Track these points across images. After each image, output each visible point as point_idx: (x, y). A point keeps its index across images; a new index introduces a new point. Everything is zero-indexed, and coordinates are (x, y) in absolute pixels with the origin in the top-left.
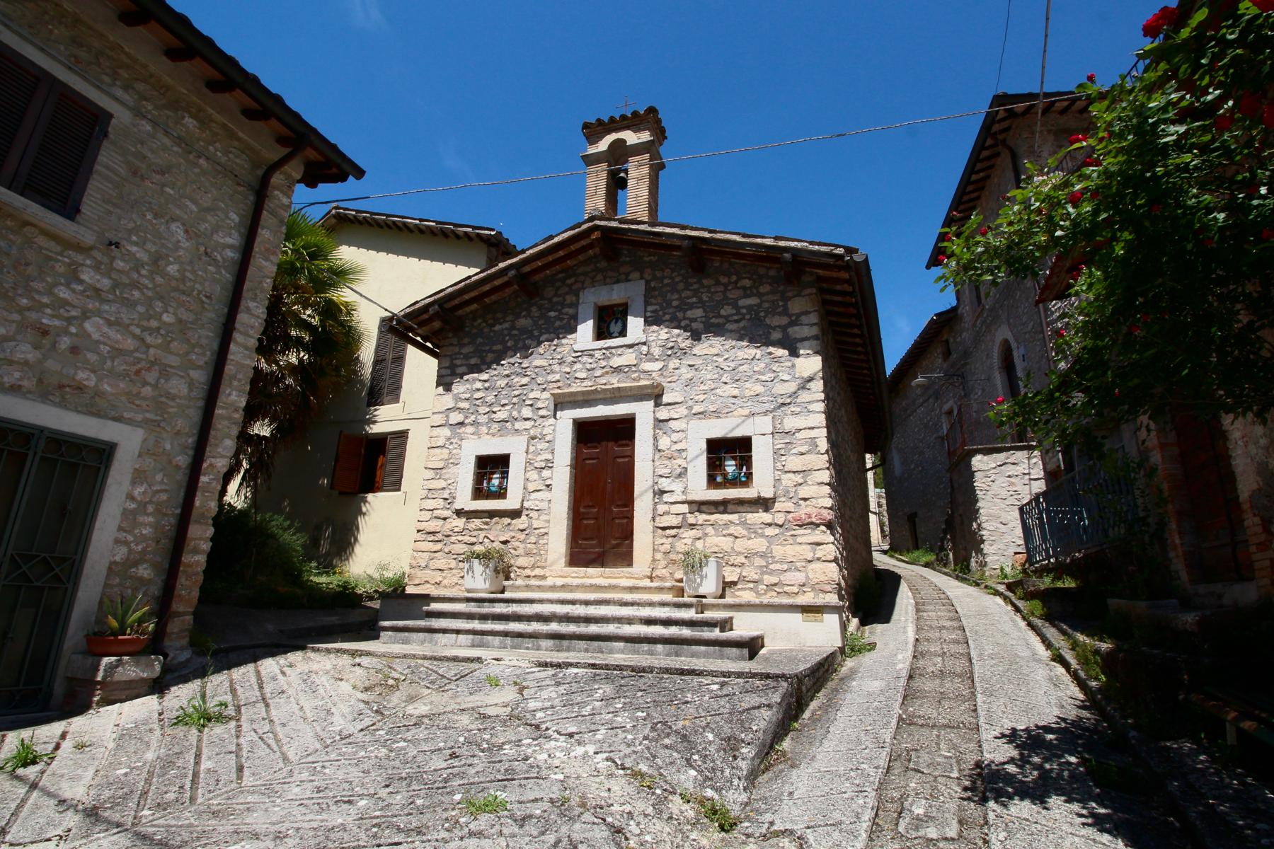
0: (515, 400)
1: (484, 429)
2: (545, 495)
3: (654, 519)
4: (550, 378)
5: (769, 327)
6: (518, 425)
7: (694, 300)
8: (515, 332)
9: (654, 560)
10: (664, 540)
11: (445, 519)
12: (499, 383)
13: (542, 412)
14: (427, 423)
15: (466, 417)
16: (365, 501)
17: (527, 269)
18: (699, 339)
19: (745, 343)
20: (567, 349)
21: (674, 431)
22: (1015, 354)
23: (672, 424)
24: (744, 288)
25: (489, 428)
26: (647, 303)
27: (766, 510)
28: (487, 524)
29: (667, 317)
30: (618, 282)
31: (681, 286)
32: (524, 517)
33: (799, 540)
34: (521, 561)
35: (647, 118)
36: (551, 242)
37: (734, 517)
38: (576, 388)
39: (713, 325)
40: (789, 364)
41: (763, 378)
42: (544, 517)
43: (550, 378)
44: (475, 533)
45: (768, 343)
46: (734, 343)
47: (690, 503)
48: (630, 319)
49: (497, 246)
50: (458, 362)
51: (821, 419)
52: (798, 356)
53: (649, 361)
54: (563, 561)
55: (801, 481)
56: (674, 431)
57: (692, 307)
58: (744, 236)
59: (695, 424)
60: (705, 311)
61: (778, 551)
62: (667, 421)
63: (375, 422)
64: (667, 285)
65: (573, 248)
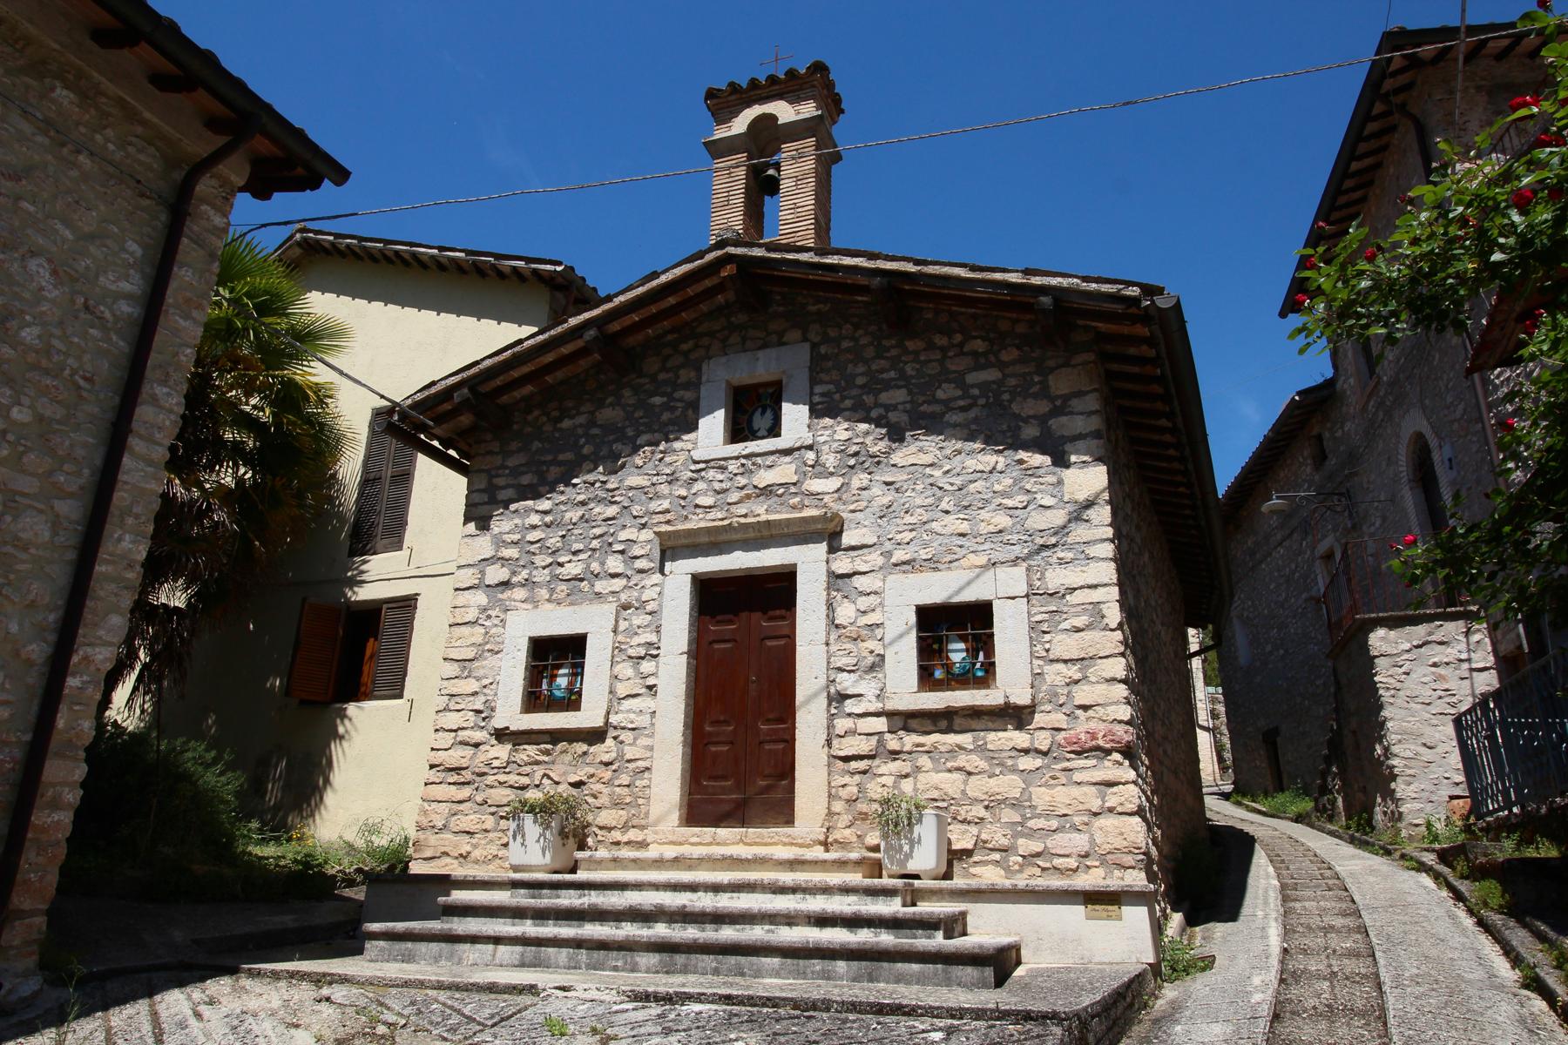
0: (595, 544)
2: (645, 703)
3: (829, 743)
4: (654, 506)
5: (1017, 417)
6: (600, 586)
7: (892, 374)
8: (595, 431)
9: (830, 814)
10: (847, 779)
11: (477, 745)
12: (568, 515)
13: (640, 564)
15: (514, 573)
16: (343, 715)
17: (615, 327)
18: (901, 440)
19: (978, 445)
20: (682, 457)
21: (862, 594)
22: (1436, 456)
23: (858, 582)
24: (975, 354)
25: (552, 591)
26: (813, 382)
27: (1020, 726)
28: (547, 753)
29: (848, 403)
30: (765, 346)
31: (870, 352)
32: (609, 742)
33: (1077, 777)
34: (605, 817)
35: (809, 80)
37: (965, 739)
38: (696, 522)
39: (924, 416)
40: (1051, 479)
41: (1010, 503)
42: (643, 741)
43: (654, 506)
44: (528, 769)
45: (1015, 446)
46: (959, 445)
47: (890, 715)
48: (786, 407)
49: (566, 290)
50: (500, 481)
51: (1108, 572)
52: (1067, 465)
53: (818, 476)
54: (675, 817)
55: (1078, 676)
56: (862, 594)
57: (888, 386)
58: (973, 268)
59: (896, 580)
60: (910, 393)
61: (1041, 796)
62: (849, 576)
64: (848, 350)
65: (690, 292)
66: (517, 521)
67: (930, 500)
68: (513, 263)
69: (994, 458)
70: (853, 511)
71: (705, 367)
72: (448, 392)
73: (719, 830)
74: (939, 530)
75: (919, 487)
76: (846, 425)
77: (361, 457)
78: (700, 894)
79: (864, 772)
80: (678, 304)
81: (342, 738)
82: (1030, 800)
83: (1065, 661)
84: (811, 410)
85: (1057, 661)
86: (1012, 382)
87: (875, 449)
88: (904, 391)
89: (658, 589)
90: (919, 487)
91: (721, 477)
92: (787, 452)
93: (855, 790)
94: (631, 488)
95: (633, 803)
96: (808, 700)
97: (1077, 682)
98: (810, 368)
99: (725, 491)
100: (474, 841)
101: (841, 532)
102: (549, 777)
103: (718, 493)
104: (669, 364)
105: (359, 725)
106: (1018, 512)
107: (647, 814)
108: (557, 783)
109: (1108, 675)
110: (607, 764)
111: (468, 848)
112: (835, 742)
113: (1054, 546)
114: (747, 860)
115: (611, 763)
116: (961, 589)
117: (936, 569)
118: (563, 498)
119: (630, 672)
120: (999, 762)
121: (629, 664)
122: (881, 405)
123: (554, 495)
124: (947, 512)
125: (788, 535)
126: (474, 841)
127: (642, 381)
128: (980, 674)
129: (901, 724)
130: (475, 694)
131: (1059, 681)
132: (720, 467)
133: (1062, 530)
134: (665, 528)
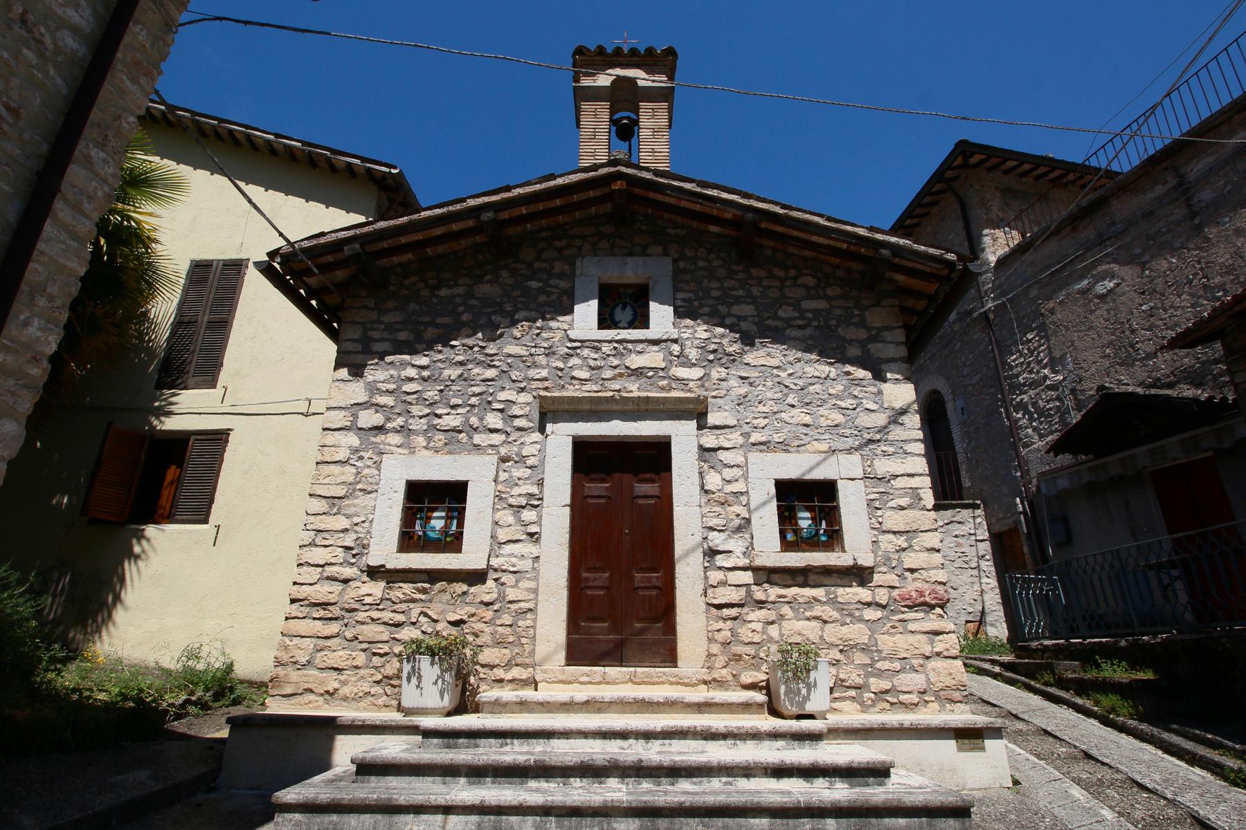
0: (474, 400)
1: (421, 441)
2: (529, 549)
4: (532, 373)
5: (843, 339)
6: (478, 439)
7: (741, 292)
9: (710, 655)
10: (720, 625)
11: (346, 581)
12: (446, 373)
14: (316, 423)
15: (388, 419)
16: (141, 536)
17: (505, 215)
18: (752, 345)
19: (814, 357)
20: (559, 335)
21: (726, 466)
22: (949, 406)
23: (722, 455)
24: (806, 286)
25: (429, 439)
26: (676, 289)
28: (424, 591)
29: (706, 310)
30: (631, 254)
31: (721, 273)
32: (490, 583)
33: (911, 627)
34: (486, 656)
36: (552, 183)
37: (819, 592)
38: (571, 392)
39: (769, 328)
40: (874, 390)
41: (843, 404)
43: (532, 373)
44: (404, 606)
45: (844, 360)
46: (799, 354)
47: (756, 570)
48: (654, 306)
49: (390, 193)
51: (921, 465)
52: (885, 380)
53: (683, 365)
54: (562, 655)
55: (905, 545)
56: (726, 466)
57: (738, 301)
58: (829, 219)
59: (755, 457)
60: (757, 309)
61: (886, 642)
62: (714, 450)
63: (171, 413)
64: (702, 268)
65: (575, 198)
66: (392, 372)
67: (779, 395)
68: (349, 159)
69: (827, 368)
70: (715, 397)
72: (338, 245)
73: (608, 669)
74: (788, 420)
75: (769, 384)
76: (705, 327)
77: (176, 301)
78: (631, 741)
79: (735, 619)
80: (562, 207)
81: (137, 557)
82: (876, 644)
83: (895, 533)
84: (675, 312)
85: (889, 532)
86: (838, 312)
87: (731, 349)
88: (752, 307)
89: (538, 447)
90: (769, 384)
91: (596, 356)
92: (656, 342)
93: (729, 634)
94: (510, 356)
95: (519, 642)
96: (687, 554)
97: (904, 550)
100: (342, 678)
101: (706, 413)
102: (426, 615)
103: (592, 368)
104: (544, 256)
105: (156, 546)
106: (849, 412)
108: (436, 621)
109: (929, 545)
110: (487, 604)
111: (336, 685)
112: (710, 591)
113: (879, 441)
114: (658, 703)
115: (492, 604)
116: (812, 469)
117: (787, 451)
118: (441, 357)
119: (511, 519)
120: (848, 613)
121: (509, 511)
122: (733, 316)
123: (431, 353)
124: (793, 406)
125: (662, 411)
127: (519, 266)
128: (823, 538)
129: (765, 578)
131: (891, 548)
132: (593, 348)
133: (883, 429)
134: (543, 393)
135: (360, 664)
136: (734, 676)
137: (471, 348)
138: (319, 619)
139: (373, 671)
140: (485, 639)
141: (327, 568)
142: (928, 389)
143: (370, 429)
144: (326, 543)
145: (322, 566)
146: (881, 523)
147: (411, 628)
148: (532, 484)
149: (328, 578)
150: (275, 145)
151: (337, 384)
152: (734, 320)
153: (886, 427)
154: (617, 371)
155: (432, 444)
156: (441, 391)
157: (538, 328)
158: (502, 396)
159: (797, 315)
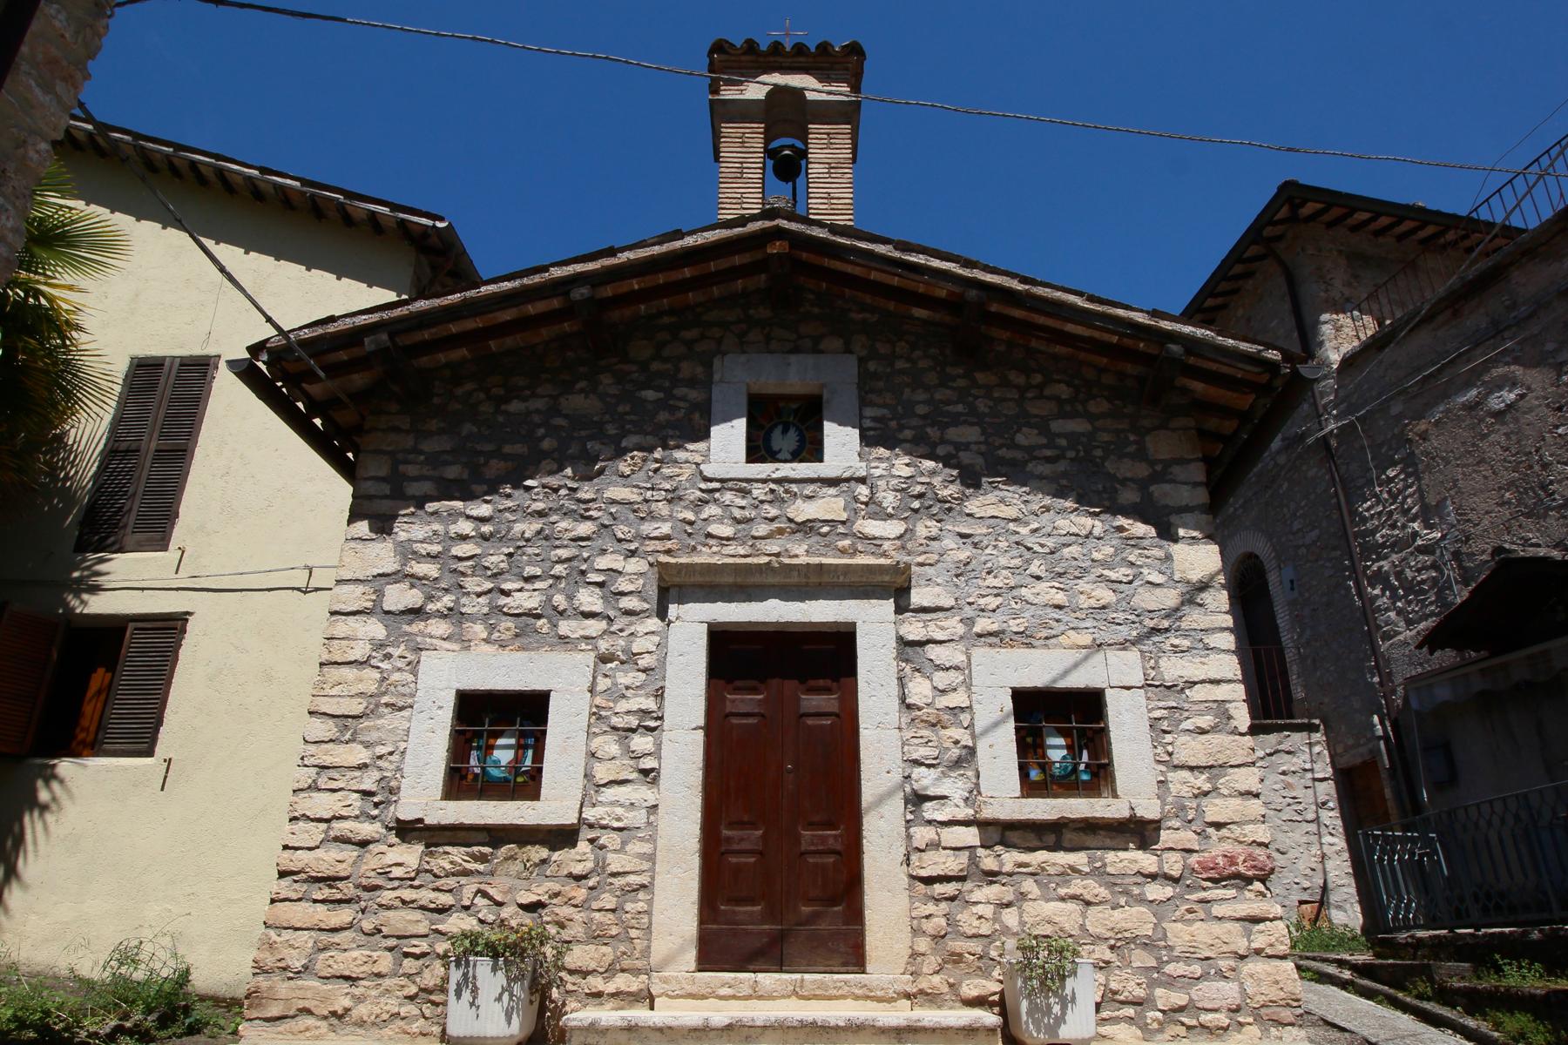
0: (559, 569)
1: (479, 630)
2: (641, 793)
3: (908, 862)
4: (647, 528)
5: (1112, 477)
6: (565, 627)
7: (960, 408)
8: (560, 421)
9: (914, 955)
10: (931, 908)
11: (363, 844)
12: (518, 527)
13: (625, 603)
14: (319, 604)
16: (50, 776)
17: (608, 291)
19: (1069, 504)
20: (687, 471)
21: (939, 668)
22: (1272, 578)
23: (933, 652)
24: (1057, 399)
25: (492, 628)
26: (863, 402)
27: (1144, 845)
28: (483, 858)
29: (908, 434)
30: (796, 350)
31: (932, 378)
32: (583, 846)
33: (1217, 910)
34: (578, 956)
35: (840, 61)
36: (678, 244)
37: (1079, 859)
38: (704, 557)
39: (1002, 461)
40: (1159, 553)
41: (1113, 575)
42: (637, 847)
43: (647, 528)
44: (451, 882)
45: (1114, 509)
46: (1048, 501)
47: (983, 825)
48: (830, 428)
49: (433, 257)
50: (412, 470)
51: (1230, 666)
52: (1175, 539)
53: (873, 516)
54: (691, 955)
55: (1207, 787)
56: (939, 668)
57: (956, 420)
58: (1091, 299)
59: (982, 655)
61: (1179, 934)
63: (95, 589)
64: (902, 372)
65: (712, 266)
66: (436, 526)
67: (1017, 562)
68: (372, 207)
69: (1089, 521)
70: (921, 565)
71: (717, 363)
73: (760, 976)
75: (1003, 545)
76: (907, 460)
77: (108, 418)
79: (952, 899)
80: (693, 279)
81: (44, 808)
82: (1165, 937)
83: (1191, 769)
84: (862, 437)
85: (1182, 767)
86: (1105, 437)
87: (946, 493)
88: (977, 429)
89: (656, 639)
90: (1003, 545)
91: (743, 503)
92: (833, 482)
93: (943, 922)
94: (614, 502)
95: (626, 937)
96: (881, 800)
97: (1206, 794)
98: (860, 388)
99: (749, 520)
100: (357, 991)
101: (909, 588)
102: (485, 895)
103: (738, 521)
104: (666, 352)
105: (74, 790)
106: (1122, 587)
107: (646, 952)
108: (500, 904)
109: (1243, 788)
110: (578, 878)
111: (347, 1002)
112: (914, 857)
113: (1167, 630)
114: (837, 1028)
115: (585, 877)
116: (1066, 673)
117: (1030, 645)
119: (614, 749)
120: (1122, 889)
123: (496, 498)
124: (1038, 578)
125: (843, 586)
126: (357, 991)
127: (626, 367)
128: (1085, 777)
129: (996, 837)
130: (363, 767)
131: (1185, 791)
133: (1173, 613)
135: (384, 970)
136: (951, 986)
137: (556, 491)
138: (323, 901)
139: (404, 981)
140: (575, 930)
141: (335, 824)
142: (1242, 551)
143: (403, 613)
144: (334, 785)
145: (328, 821)
146: (1170, 754)
147: (462, 915)
148: (647, 696)
149: (336, 839)
150: (262, 185)
151: (352, 544)
152: (951, 449)
153: (1177, 610)
154: (776, 525)
155: (496, 635)
156: (510, 555)
157: (656, 461)
158: (603, 562)
159: (1045, 441)
